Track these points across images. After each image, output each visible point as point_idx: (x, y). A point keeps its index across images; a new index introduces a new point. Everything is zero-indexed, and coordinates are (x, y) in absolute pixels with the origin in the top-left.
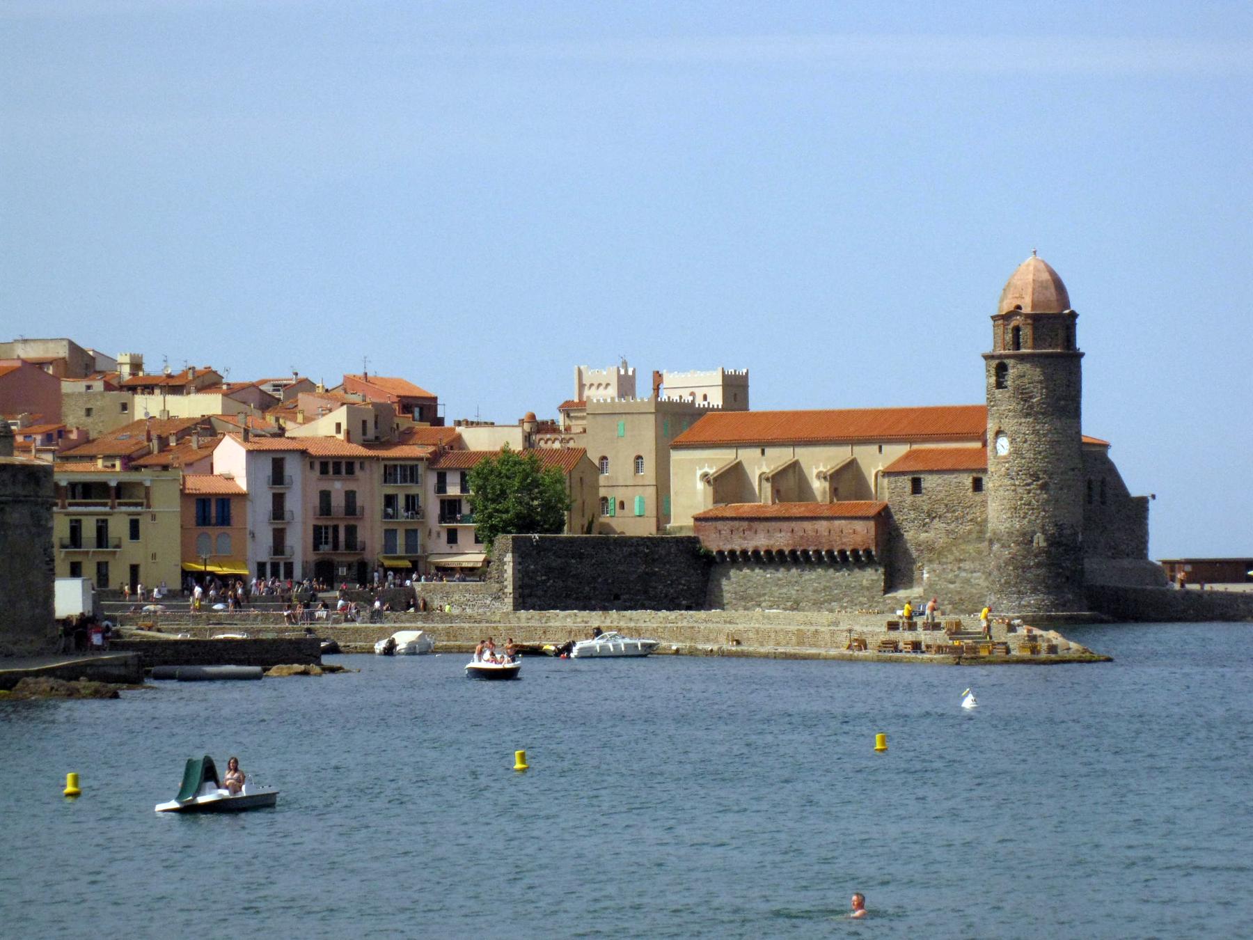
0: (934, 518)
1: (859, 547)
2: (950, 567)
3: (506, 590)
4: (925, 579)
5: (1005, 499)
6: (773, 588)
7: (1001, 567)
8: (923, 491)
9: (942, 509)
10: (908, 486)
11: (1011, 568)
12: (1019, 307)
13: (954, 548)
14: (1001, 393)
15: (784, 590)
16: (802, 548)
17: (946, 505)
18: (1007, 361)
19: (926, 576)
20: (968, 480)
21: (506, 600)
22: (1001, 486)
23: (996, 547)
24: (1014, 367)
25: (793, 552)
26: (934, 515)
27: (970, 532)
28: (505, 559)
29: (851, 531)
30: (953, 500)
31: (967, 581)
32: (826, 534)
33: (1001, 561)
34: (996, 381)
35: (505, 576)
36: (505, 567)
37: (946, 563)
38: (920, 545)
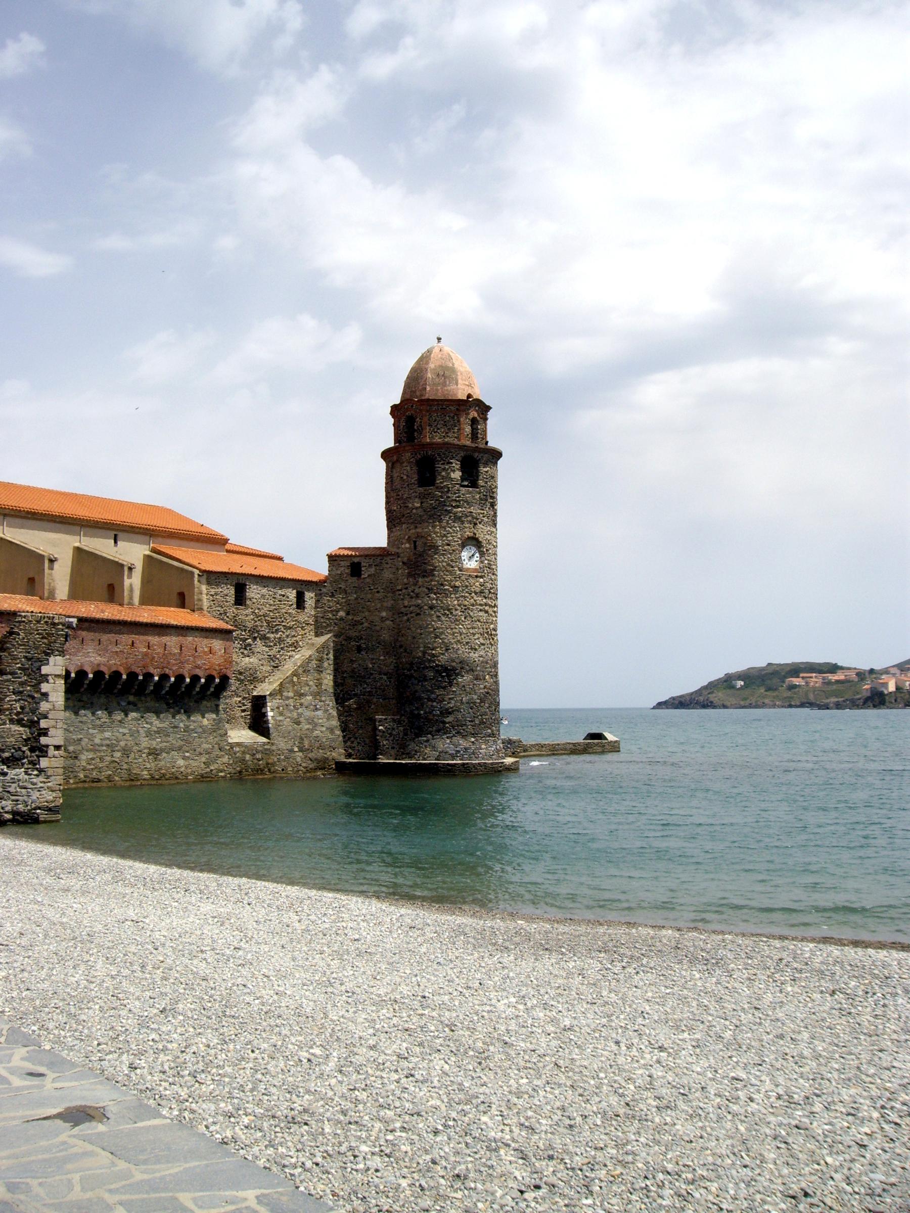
0: (255, 638)
1: (215, 673)
2: (291, 702)
3: (44, 740)
4: (270, 718)
5: (479, 621)
6: (90, 731)
7: (475, 703)
8: (248, 602)
9: (264, 630)
10: (232, 591)
11: (487, 705)
12: (469, 396)
13: (295, 679)
14: (470, 493)
15: (107, 734)
16: (144, 671)
17: (268, 622)
18: (476, 455)
19: (270, 714)
20: (292, 594)
21: (44, 763)
22: (473, 605)
23: (465, 679)
24: (486, 465)
25: (132, 675)
26: (256, 635)
27: (310, 659)
28: (45, 670)
29: (206, 650)
30: (277, 618)
31: (311, 721)
32: (177, 651)
33: (475, 697)
34: (460, 477)
35: (44, 706)
36: (45, 687)
37: (288, 698)
38: (241, 673)
